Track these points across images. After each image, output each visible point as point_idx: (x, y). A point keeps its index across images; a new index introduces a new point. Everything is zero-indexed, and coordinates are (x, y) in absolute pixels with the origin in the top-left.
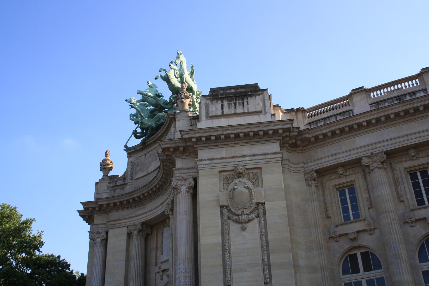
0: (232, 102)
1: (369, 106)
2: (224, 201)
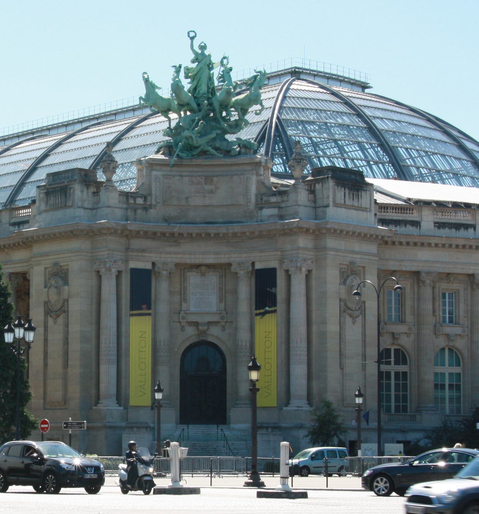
0: (352, 192)
1: (433, 225)
2: (344, 296)
